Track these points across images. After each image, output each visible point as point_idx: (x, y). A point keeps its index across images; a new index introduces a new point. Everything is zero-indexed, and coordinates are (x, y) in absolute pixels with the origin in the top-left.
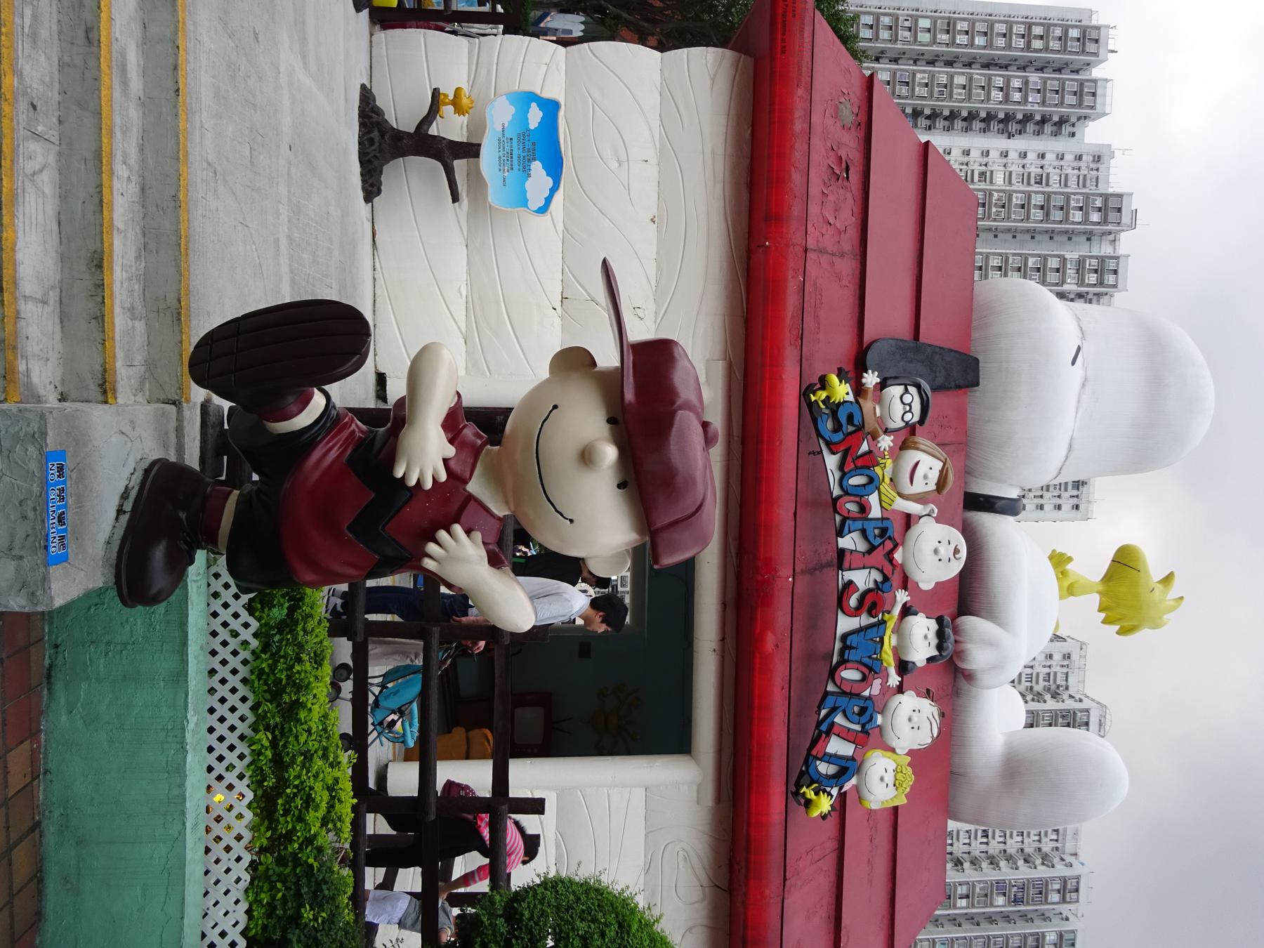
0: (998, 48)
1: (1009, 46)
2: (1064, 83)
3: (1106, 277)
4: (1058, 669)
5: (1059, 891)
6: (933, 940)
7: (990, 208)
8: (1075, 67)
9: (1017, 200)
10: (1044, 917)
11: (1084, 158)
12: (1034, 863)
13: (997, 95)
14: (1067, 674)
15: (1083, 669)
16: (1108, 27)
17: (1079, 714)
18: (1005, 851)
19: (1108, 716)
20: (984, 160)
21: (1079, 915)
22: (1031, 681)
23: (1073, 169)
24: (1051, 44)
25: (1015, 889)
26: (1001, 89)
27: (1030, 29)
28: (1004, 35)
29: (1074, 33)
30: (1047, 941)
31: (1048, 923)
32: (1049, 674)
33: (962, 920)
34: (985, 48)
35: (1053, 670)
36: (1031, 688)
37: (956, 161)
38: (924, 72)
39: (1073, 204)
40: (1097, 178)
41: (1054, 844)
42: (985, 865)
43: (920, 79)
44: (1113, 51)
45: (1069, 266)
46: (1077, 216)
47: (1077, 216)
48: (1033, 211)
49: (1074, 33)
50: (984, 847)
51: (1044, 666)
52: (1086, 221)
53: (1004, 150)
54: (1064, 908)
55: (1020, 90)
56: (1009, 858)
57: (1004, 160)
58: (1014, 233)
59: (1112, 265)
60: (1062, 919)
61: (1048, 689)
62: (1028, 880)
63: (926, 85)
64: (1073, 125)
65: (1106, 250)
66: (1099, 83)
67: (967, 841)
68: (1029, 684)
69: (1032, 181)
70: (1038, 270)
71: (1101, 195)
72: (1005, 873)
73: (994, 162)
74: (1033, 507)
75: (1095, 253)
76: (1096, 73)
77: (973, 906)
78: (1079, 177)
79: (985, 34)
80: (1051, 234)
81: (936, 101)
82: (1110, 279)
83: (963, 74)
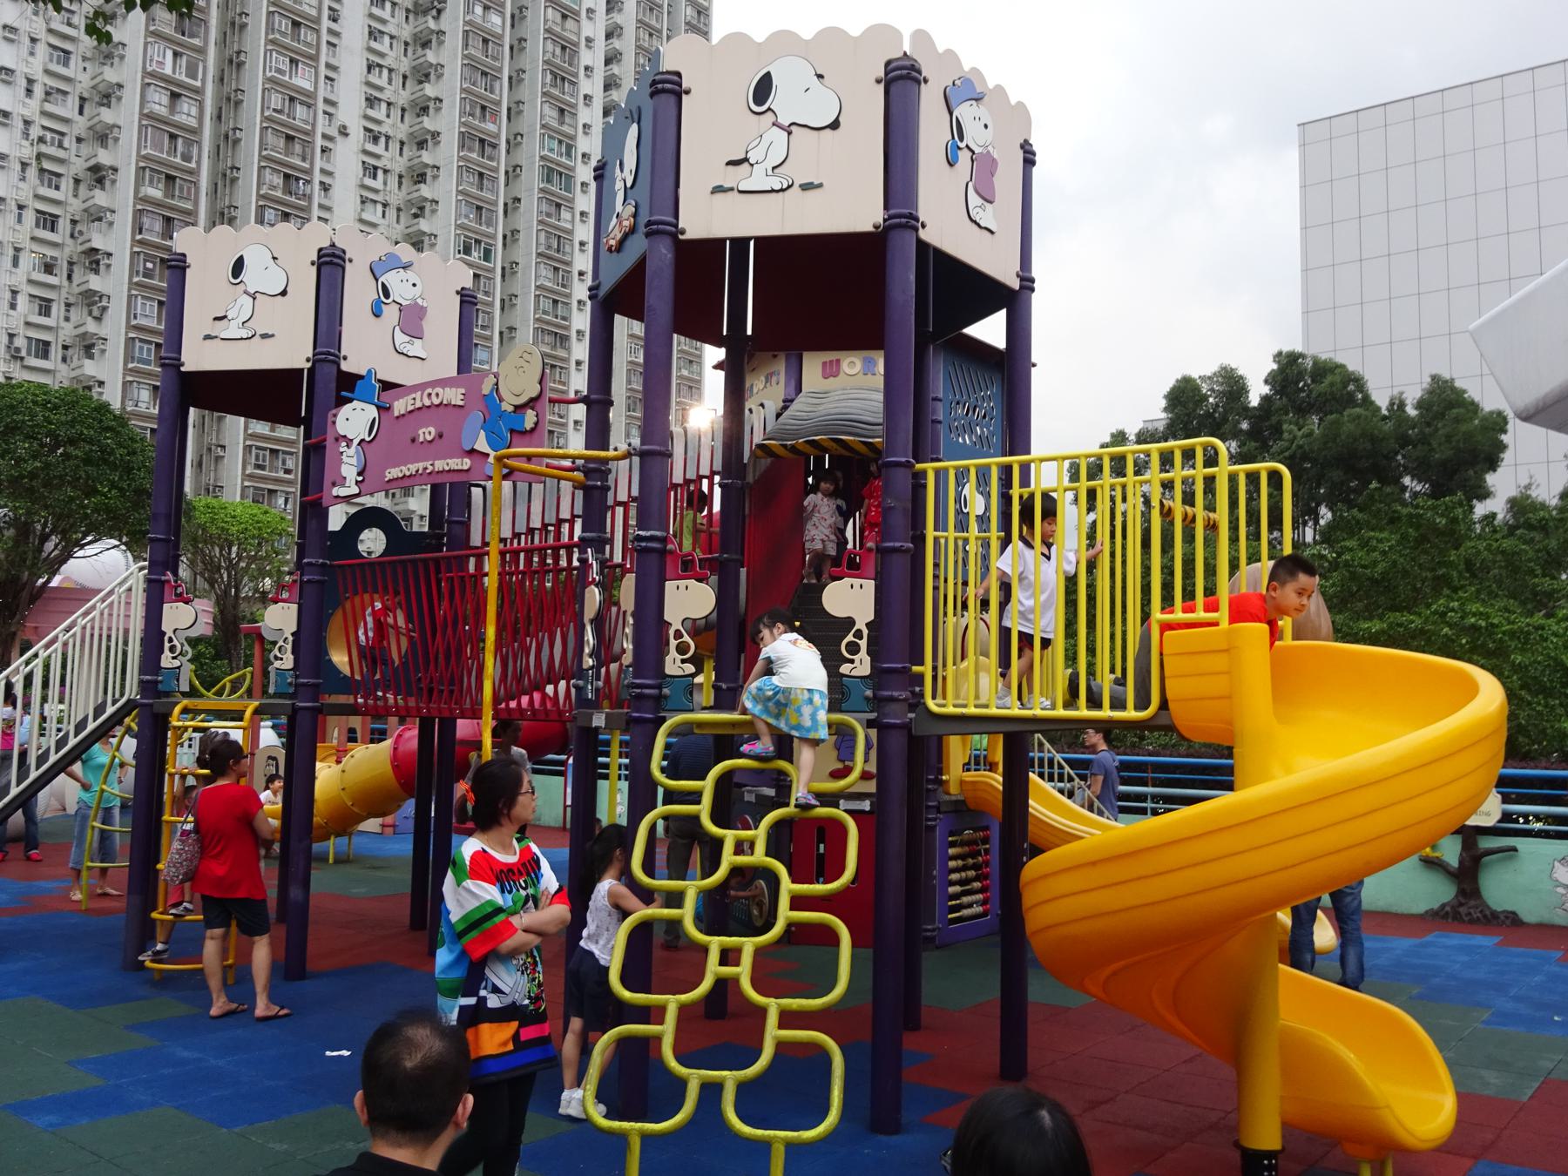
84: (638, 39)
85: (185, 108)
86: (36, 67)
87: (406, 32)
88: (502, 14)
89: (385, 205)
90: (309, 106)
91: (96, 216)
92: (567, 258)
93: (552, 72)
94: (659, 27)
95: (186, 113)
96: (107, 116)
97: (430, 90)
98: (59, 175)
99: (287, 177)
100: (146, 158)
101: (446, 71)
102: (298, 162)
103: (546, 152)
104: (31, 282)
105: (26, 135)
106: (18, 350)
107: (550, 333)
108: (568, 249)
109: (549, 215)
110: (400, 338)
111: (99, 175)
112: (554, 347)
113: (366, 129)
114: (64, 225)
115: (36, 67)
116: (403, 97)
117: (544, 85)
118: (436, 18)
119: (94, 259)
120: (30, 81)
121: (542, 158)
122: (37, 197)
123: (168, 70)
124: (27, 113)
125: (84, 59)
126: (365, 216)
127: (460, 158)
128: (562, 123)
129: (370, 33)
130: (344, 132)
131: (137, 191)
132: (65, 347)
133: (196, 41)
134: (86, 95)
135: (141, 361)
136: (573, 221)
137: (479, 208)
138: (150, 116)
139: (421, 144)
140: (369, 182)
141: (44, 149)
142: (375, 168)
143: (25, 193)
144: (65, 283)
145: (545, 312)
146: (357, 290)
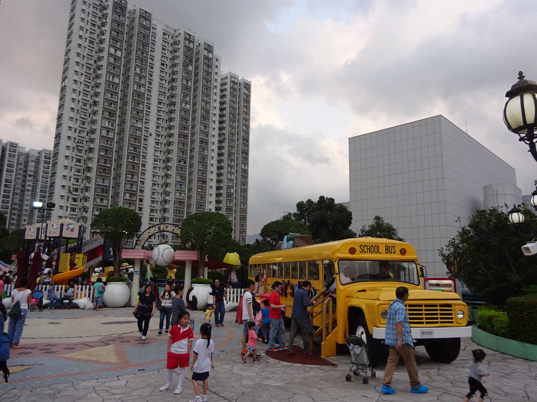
6: (202, 100)
10: (198, 53)
12: (177, 49)
18: (171, 59)
22: (96, 17)
31: (200, 52)
32: (94, 7)
36: (99, 18)
50: (168, 67)
54: (196, 44)
56: (174, 58)
60: (199, 46)
61: (101, 11)
62: (184, 53)
72: (180, 61)
77: (191, 79)
84: (230, 104)
86: (77, 126)
87: (167, 110)
88: (190, 105)
90: (140, 131)
91: (90, 159)
92: (206, 162)
95: (111, 135)
96: (93, 136)
97: (172, 124)
98: (82, 150)
99: (135, 148)
100: (101, 146)
101: (176, 119)
102: (137, 144)
104: (74, 175)
105: (74, 141)
106: (71, 190)
107: (201, 181)
108: (206, 160)
109: (201, 152)
110: (70, 232)
111: (91, 150)
112: (202, 184)
114: (82, 161)
115: (77, 126)
116: (166, 125)
117: (201, 120)
118: (174, 107)
119: (89, 169)
120: (76, 129)
121: (200, 138)
122: (76, 155)
123: (107, 126)
124: (74, 136)
125: (88, 123)
126: (155, 154)
127: (178, 140)
128: (205, 129)
129: (158, 111)
130: (151, 135)
132: (82, 189)
133: (113, 118)
134: (89, 131)
136: (208, 153)
138: (102, 136)
139: (170, 137)
141: (78, 144)
142: (159, 143)
143: (74, 154)
144: (82, 175)
145: (200, 176)
146: (65, 228)
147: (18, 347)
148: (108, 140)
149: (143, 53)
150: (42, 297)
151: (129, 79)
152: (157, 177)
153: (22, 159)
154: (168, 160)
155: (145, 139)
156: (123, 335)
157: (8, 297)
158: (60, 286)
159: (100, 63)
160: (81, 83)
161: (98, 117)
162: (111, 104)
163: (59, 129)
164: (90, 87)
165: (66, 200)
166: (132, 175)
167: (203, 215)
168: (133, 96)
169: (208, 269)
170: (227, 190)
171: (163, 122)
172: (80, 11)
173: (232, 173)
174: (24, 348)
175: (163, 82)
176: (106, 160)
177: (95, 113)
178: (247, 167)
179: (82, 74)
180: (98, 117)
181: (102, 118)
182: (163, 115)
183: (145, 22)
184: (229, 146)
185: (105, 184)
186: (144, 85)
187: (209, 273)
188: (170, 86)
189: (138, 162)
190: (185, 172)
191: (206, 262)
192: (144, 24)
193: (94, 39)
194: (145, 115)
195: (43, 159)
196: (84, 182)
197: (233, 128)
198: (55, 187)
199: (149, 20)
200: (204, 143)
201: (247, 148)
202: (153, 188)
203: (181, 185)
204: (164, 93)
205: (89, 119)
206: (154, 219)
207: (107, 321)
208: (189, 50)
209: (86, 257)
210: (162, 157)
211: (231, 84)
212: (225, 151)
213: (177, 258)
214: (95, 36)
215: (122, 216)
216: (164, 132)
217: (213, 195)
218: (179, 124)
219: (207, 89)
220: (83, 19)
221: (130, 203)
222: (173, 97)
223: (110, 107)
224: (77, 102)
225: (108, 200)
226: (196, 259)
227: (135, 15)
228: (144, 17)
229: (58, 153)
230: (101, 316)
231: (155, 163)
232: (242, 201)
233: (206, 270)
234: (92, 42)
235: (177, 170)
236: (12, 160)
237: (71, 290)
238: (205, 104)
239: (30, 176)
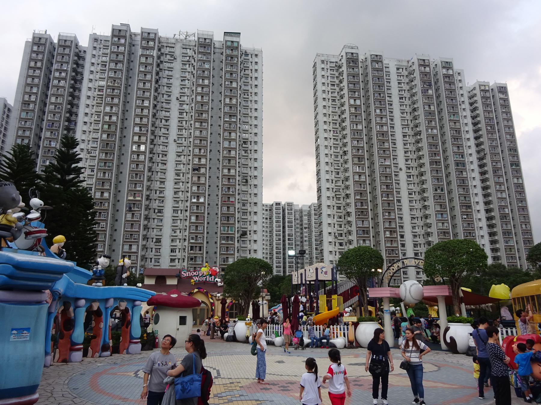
0: (39, 82)
1: (39, 77)
2: (59, 54)
3: (151, 37)
4: (328, 66)
5: (425, 68)
6: (449, 120)
7: (115, 87)
8: (52, 50)
9: (112, 74)
10: (436, 75)
11: (95, 46)
12: (413, 78)
13: (62, 83)
14: (330, 62)
15: (328, 56)
16: (34, 34)
17: (348, 57)
18: (408, 90)
19: (349, 45)
20: (93, 89)
21: (434, 61)
22: (334, 77)
23: (100, 51)
24: (40, 58)
25: (425, 86)
26: (59, 81)
27: (31, 67)
28: (33, 79)
29: (35, 48)
30: (446, 73)
31: (438, 73)
32: (331, 70)
33: (439, 108)
34: (38, 88)
35: (329, 68)
36: (337, 77)
37: (92, 102)
38: (48, 116)
39: (116, 50)
40: (105, 41)
41: (404, 70)
42: (415, 98)
43: (51, 117)
44: (46, 32)
45: (145, 53)
46: (122, 49)
47: (122, 49)
48: (118, 68)
49: (35, 48)
50: (407, 99)
51: (327, 71)
52: (124, 45)
53: (89, 80)
54: (432, 66)
55: (60, 73)
56: (411, 88)
57: (94, 81)
58: (128, 78)
59: (145, 35)
60: (436, 67)
61: (337, 70)
62: (421, 80)
63: (54, 115)
64: (80, 51)
65: (139, 38)
66: (60, 38)
67: (405, 106)
68: (335, 78)
69: (104, 68)
70: (146, 66)
71: (112, 38)
72: (418, 89)
73: (94, 85)
74: (256, 74)
75: (140, 42)
76: (56, 41)
77: (433, 103)
78: (104, 49)
79: (32, 87)
80: (130, 61)
81: (62, 111)
82: (152, 36)
83: (50, 98)
84: (484, 116)
85: (362, 177)
86: (333, 177)
87: (413, 141)
88: (437, 129)
89: (414, 184)
90: (390, 168)
91: (348, 204)
93: (454, 138)
94: (491, 110)
95: (363, 178)
96: (347, 183)
98: (340, 198)
100: (356, 190)
101: (424, 148)
102: (389, 181)
103: (455, 159)
105: (333, 191)
107: (464, 206)
108: (466, 182)
109: (459, 175)
111: (348, 196)
112: (467, 209)
113: (406, 167)
114: (342, 208)
115: (333, 177)
116: (415, 156)
117: (452, 142)
118: (420, 135)
119: (349, 214)
120: (332, 180)
121: (455, 161)
123: (358, 171)
124: (332, 187)
126: (409, 188)
127: (430, 168)
128: (459, 150)
130: (401, 169)
131: (354, 198)
133: (363, 163)
135: (360, 234)
136: (467, 174)
137: (438, 179)
138: (356, 181)
139: (421, 167)
140: (409, 179)
141: (337, 193)
142: (410, 175)
143: (334, 203)
145: (462, 201)
147: (263, 383)
148: (360, 183)
149: (380, 94)
150: (302, 336)
151: (371, 122)
152: (415, 210)
153: (297, 215)
154: (424, 191)
155: (396, 175)
156: (361, 378)
157: (279, 336)
158: (318, 326)
159: (343, 116)
160: (330, 139)
161: (349, 165)
162: (358, 150)
163: (319, 183)
164: (339, 140)
165: (334, 245)
166: (389, 213)
167: (447, 244)
168: (377, 137)
169: (465, 305)
170: (500, 211)
171: (411, 154)
172: (321, 77)
173: (502, 192)
174: (269, 384)
175: (405, 115)
176: (362, 203)
177: (346, 162)
178: (520, 180)
179: (330, 131)
180: (349, 165)
181: (353, 164)
182: (411, 147)
183: (377, 65)
184: (493, 161)
185: (365, 226)
186: (386, 124)
187: (467, 310)
188: (412, 117)
189: (392, 199)
190: (444, 200)
191: (462, 297)
192: (377, 67)
193: (335, 97)
194: (391, 151)
195: (313, 212)
196: (347, 226)
197: (493, 140)
198: (324, 234)
199: (381, 61)
200: (461, 165)
201: (516, 158)
202: (413, 222)
203: (442, 214)
204: (407, 125)
205: (342, 168)
206: (420, 254)
207: (353, 362)
208: (426, 75)
209: (342, 298)
210: (417, 189)
211: (482, 93)
212: (489, 168)
213: (425, 295)
214: (336, 95)
215: (361, 256)
216: (414, 164)
217: (482, 219)
218: (428, 151)
219: (453, 107)
220: (323, 83)
221: (392, 241)
222: (417, 126)
223: (358, 153)
224: (330, 156)
225: (370, 240)
226: (448, 294)
227: (367, 62)
228: (375, 61)
229: (321, 204)
230: (352, 356)
231: (410, 196)
232: (523, 221)
233: (463, 306)
234: (334, 100)
235: (434, 199)
236: (291, 217)
237: (327, 330)
238: (453, 124)
239: (305, 228)
